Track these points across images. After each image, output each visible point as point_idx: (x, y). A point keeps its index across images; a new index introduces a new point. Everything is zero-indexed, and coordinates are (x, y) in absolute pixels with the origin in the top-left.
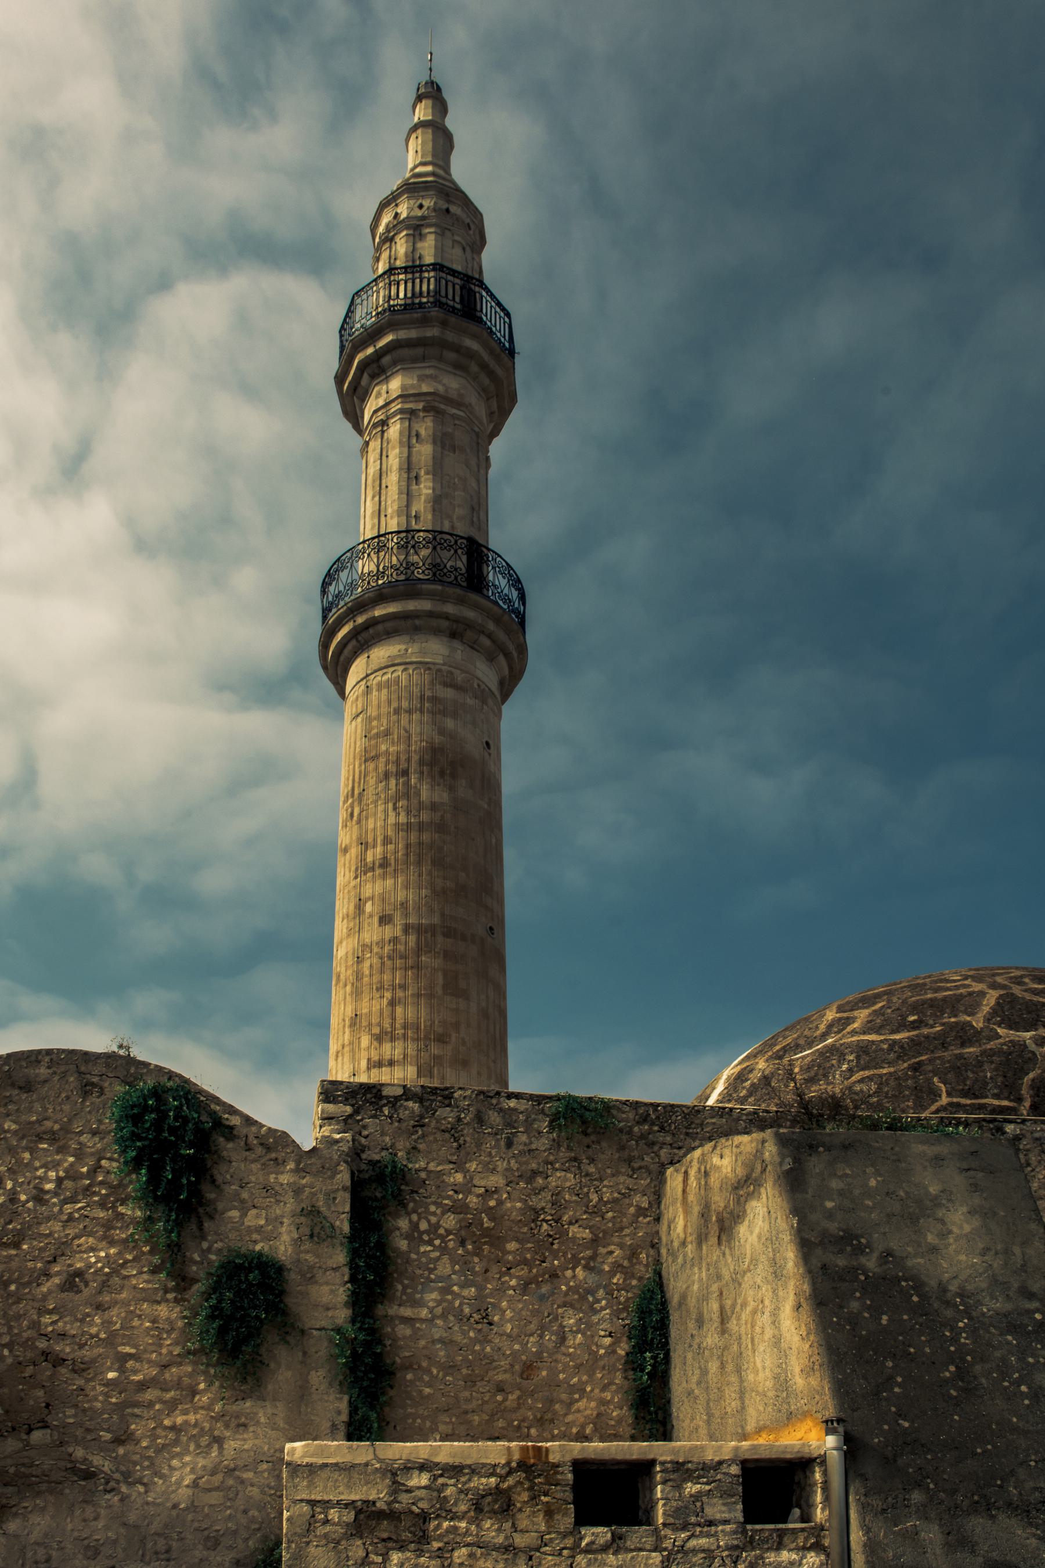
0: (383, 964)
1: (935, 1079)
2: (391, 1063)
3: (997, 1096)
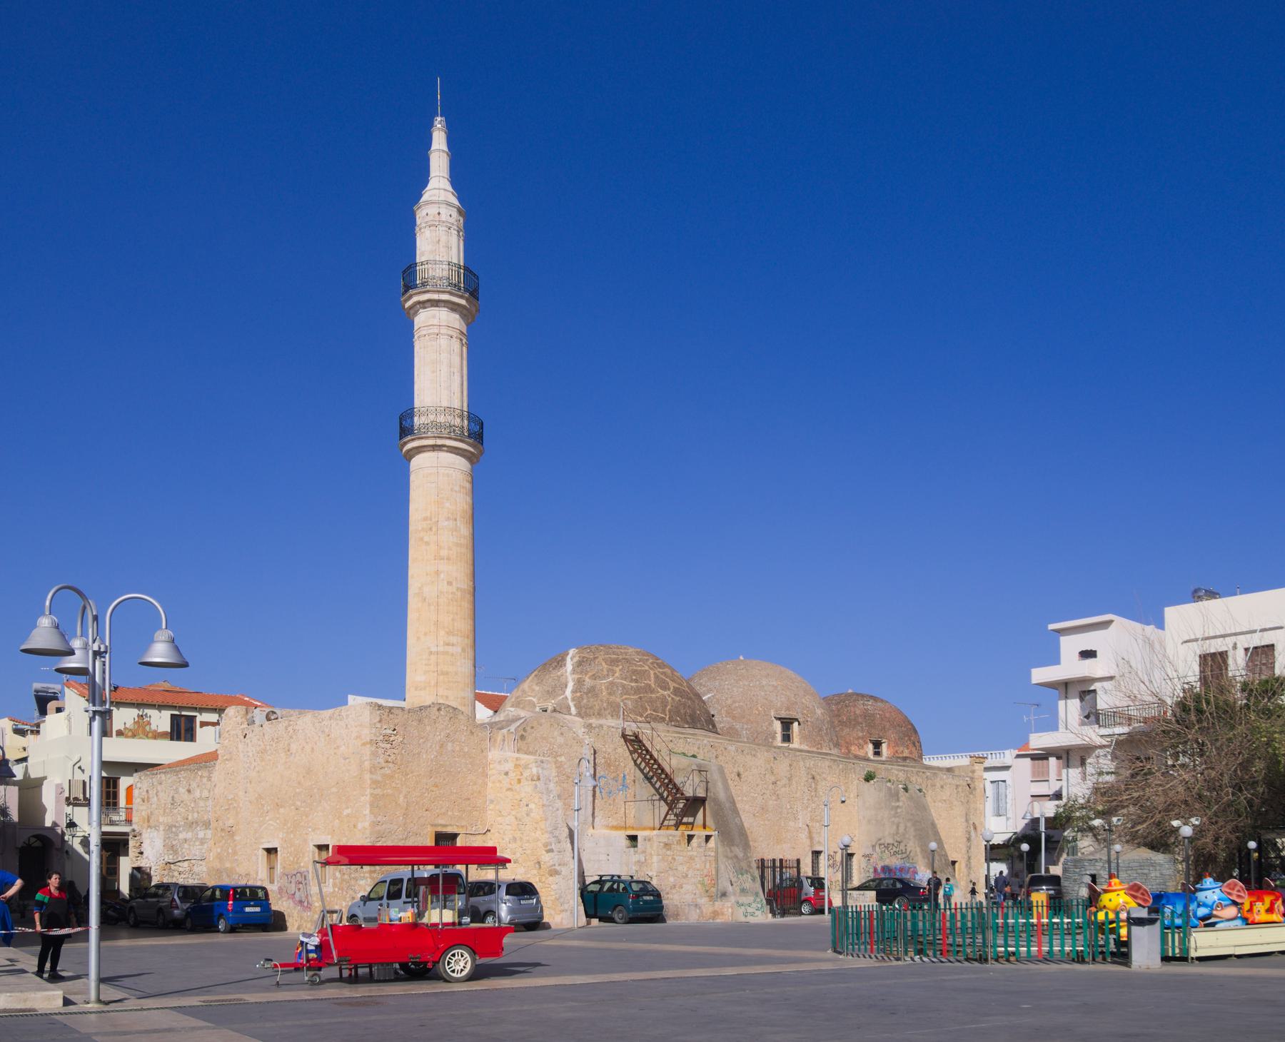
3: (661, 713)
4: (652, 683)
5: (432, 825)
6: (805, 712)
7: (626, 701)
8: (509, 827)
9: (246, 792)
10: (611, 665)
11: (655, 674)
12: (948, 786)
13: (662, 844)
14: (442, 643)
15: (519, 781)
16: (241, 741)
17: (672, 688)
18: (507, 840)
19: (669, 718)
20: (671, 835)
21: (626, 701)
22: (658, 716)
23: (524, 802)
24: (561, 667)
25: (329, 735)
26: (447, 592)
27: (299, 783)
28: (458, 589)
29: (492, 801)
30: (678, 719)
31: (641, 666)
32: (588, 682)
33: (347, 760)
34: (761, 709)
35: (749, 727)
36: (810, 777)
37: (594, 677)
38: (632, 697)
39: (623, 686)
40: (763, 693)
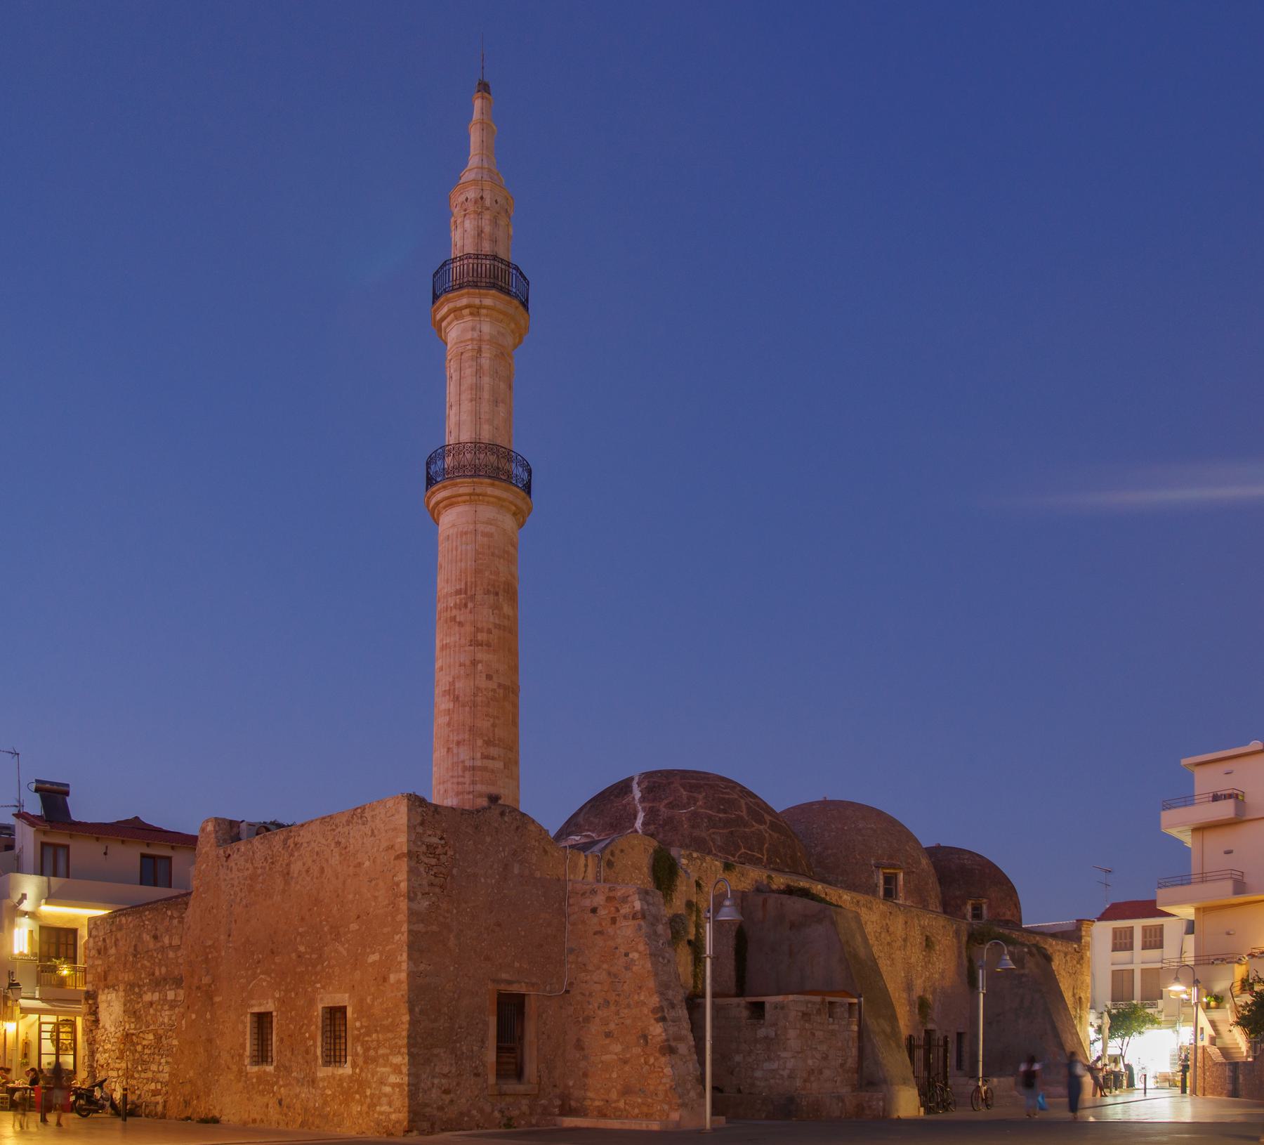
0: (489, 702)
1: (739, 841)
2: (493, 758)
3: (758, 852)
4: (744, 814)
5: (494, 981)
6: (910, 861)
7: (713, 836)
8: (598, 987)
9: (229, 936)
10: (691, 792)
11: (746, 804)
12: (1057, 953)
13: (800, 1014)
14: (479, 755)
15: (614, 921)
16: (222, 866)
17: (768, 822)
18: (596, 1005)
19: (767, 859)
20: (810, 1002)
21: (713, 836)
22: (754, 856)
23: (622, 950)
24: (626, 793)
25: (345, 848)
26: (485, 689)
27: (303, 919)
28: (500, 685)
29: (571, 951)
30: (778, 861)
31: (728, 793)
32: (664, 812)
33: (374, 882)
34: (858, 857)
35: (845, 879)
36: (925, 938)
37: (671, 806)
38: (721, 831)
39: (710, 817)
40: (860, 838)
